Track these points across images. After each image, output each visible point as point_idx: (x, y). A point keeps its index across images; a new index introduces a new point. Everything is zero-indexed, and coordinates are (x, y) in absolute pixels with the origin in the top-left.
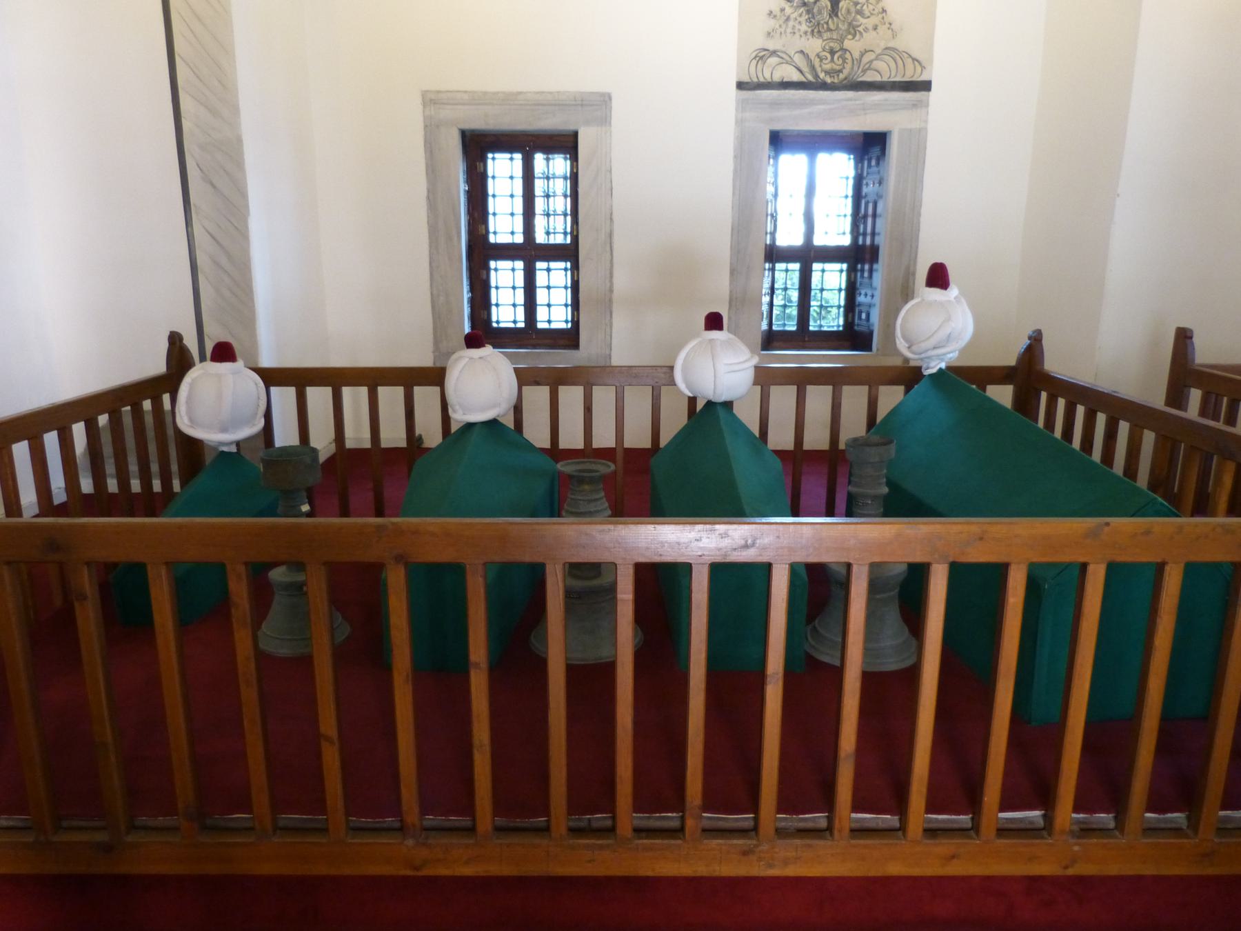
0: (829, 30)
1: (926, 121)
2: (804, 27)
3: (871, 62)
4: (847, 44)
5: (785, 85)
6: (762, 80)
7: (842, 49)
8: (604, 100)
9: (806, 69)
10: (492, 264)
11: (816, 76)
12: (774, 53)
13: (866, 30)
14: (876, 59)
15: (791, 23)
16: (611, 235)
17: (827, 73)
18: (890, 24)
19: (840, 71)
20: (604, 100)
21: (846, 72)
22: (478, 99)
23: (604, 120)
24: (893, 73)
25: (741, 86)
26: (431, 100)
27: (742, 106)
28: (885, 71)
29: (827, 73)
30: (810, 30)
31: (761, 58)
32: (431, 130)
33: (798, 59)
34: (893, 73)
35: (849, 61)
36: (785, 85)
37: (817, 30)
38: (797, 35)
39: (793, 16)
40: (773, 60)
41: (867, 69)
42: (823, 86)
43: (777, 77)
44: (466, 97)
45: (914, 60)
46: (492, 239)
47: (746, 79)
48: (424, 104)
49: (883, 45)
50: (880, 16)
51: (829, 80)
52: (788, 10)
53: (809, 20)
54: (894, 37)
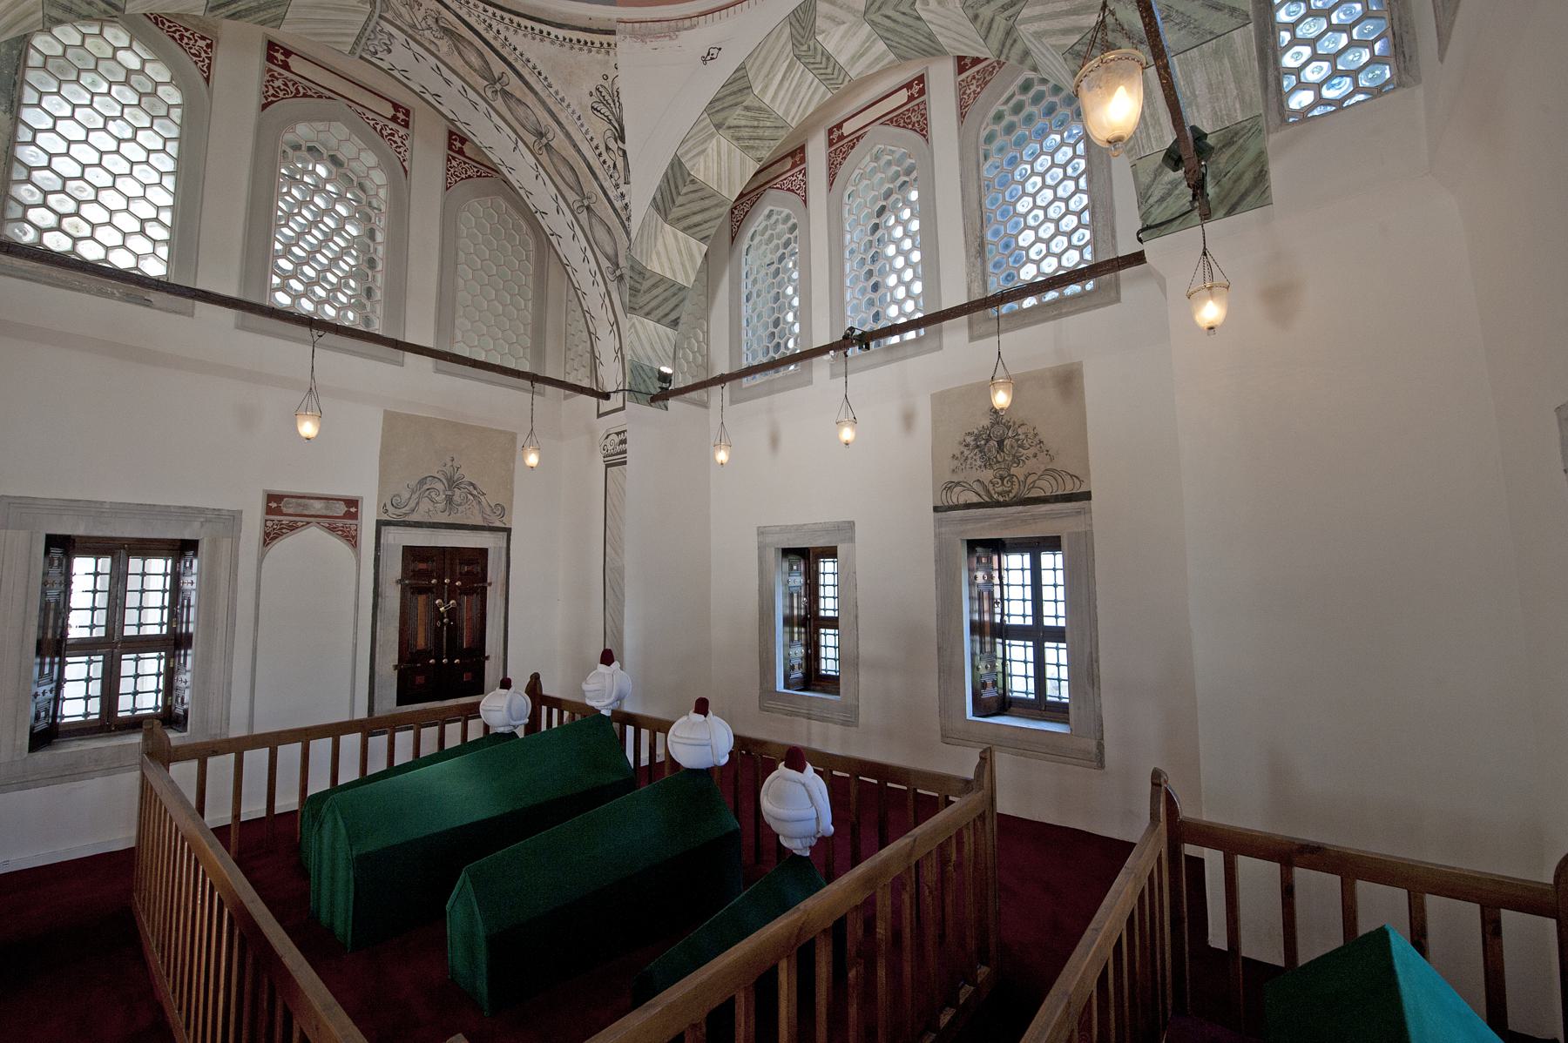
0: (998, 462)
1: (1091, 525)
2: (979, 463)
3: (1034, 482)
4: (1013, 471)
5: (968, 506)
6: (951, 504)
7: (1009, 475)
8: (851, 525)
9: (982, 493)
10: (823, 631)
11: (991, 497)
12: (958, 484)
13: (1028, 458)
14: (1039, 479)
15: (969, 462)
16: (857, 617)
17: (999, 494)
18: (1047, 451)
19: (1010, 491)
20: (851, 525)
21: (1014, 492)
22: (785, 529)
23: (852, 540)
24: (1055, 489)
25: (936, 509)
26: (761, 532)
27: (939, 523)
28: (1047, 487)
29: (999, 494)
30: (983, 464)
31: (949, 488)
32: (762, 548)
33: (975, 486)
34: (1055, 489)
35: (1016, 483)
36: (968, 506)
37: (988, 464)
38: (974, 469)
39: (970, 456)
40: (958, 489)
41: (1032, 488)
42: (998, 504)
43: (962, 501)
44: (778, 529)
45: (1071, 476)
46: (822, 613)
47: (940, 504)
48: (758, 535)
49: (1043, 467)
50: (1038, 446)
51: (1001, 499)
52: (966, 453)
53: (982, 458)
54: (1052, 459)
